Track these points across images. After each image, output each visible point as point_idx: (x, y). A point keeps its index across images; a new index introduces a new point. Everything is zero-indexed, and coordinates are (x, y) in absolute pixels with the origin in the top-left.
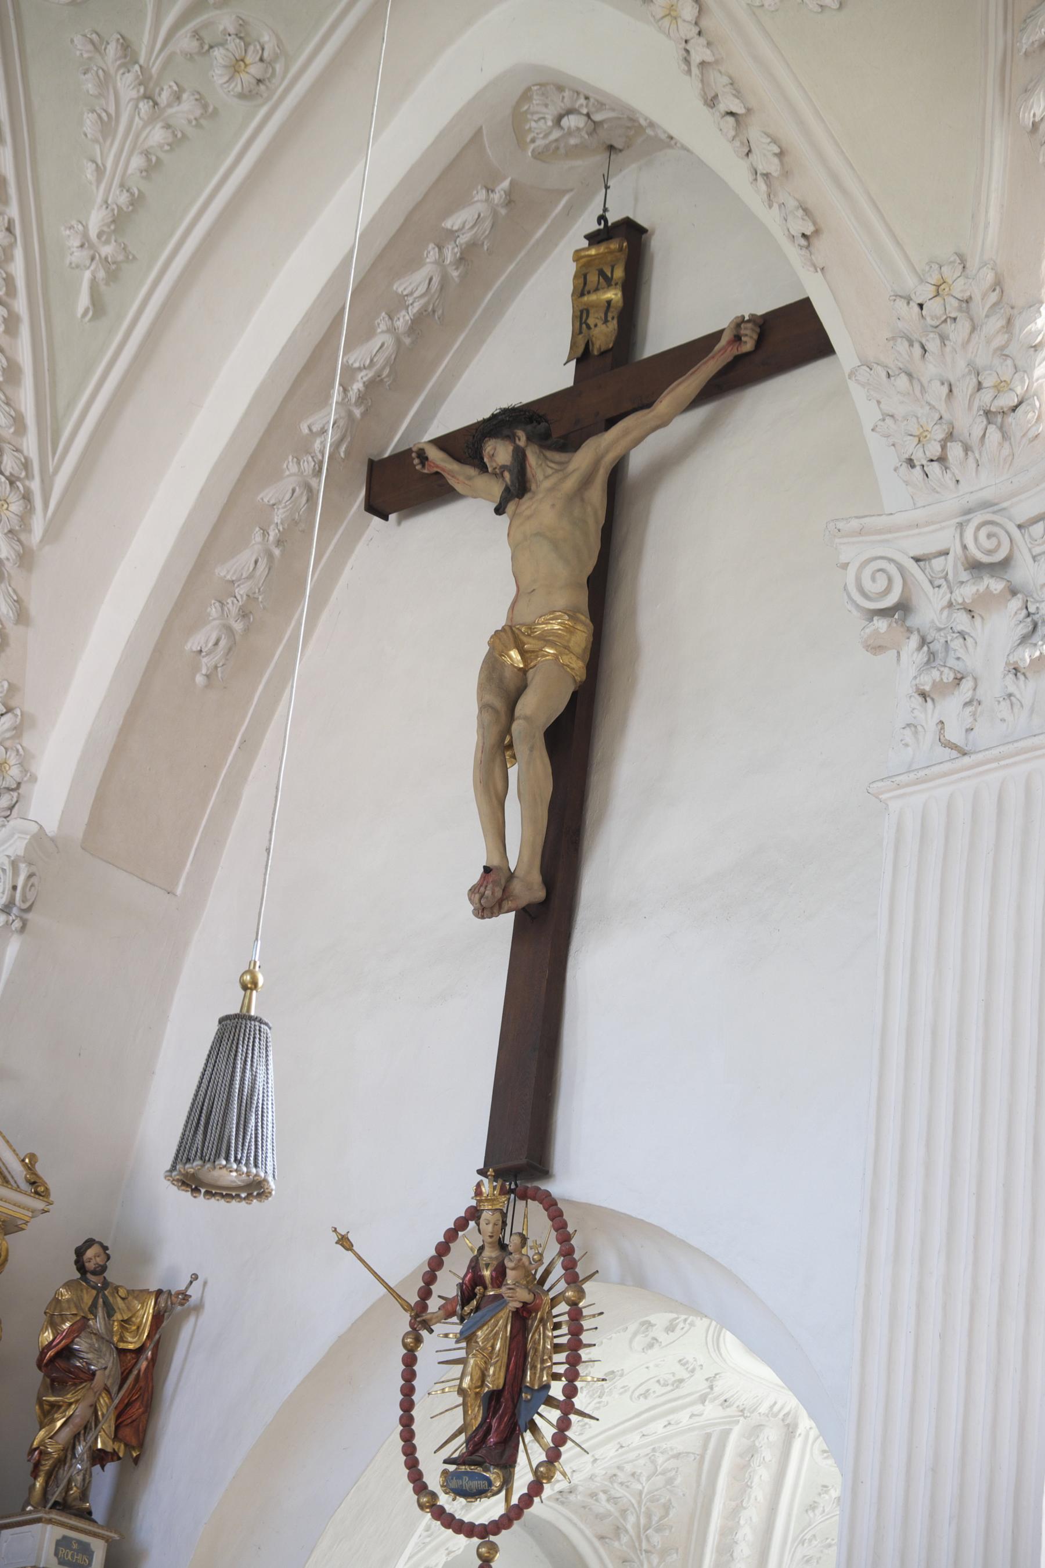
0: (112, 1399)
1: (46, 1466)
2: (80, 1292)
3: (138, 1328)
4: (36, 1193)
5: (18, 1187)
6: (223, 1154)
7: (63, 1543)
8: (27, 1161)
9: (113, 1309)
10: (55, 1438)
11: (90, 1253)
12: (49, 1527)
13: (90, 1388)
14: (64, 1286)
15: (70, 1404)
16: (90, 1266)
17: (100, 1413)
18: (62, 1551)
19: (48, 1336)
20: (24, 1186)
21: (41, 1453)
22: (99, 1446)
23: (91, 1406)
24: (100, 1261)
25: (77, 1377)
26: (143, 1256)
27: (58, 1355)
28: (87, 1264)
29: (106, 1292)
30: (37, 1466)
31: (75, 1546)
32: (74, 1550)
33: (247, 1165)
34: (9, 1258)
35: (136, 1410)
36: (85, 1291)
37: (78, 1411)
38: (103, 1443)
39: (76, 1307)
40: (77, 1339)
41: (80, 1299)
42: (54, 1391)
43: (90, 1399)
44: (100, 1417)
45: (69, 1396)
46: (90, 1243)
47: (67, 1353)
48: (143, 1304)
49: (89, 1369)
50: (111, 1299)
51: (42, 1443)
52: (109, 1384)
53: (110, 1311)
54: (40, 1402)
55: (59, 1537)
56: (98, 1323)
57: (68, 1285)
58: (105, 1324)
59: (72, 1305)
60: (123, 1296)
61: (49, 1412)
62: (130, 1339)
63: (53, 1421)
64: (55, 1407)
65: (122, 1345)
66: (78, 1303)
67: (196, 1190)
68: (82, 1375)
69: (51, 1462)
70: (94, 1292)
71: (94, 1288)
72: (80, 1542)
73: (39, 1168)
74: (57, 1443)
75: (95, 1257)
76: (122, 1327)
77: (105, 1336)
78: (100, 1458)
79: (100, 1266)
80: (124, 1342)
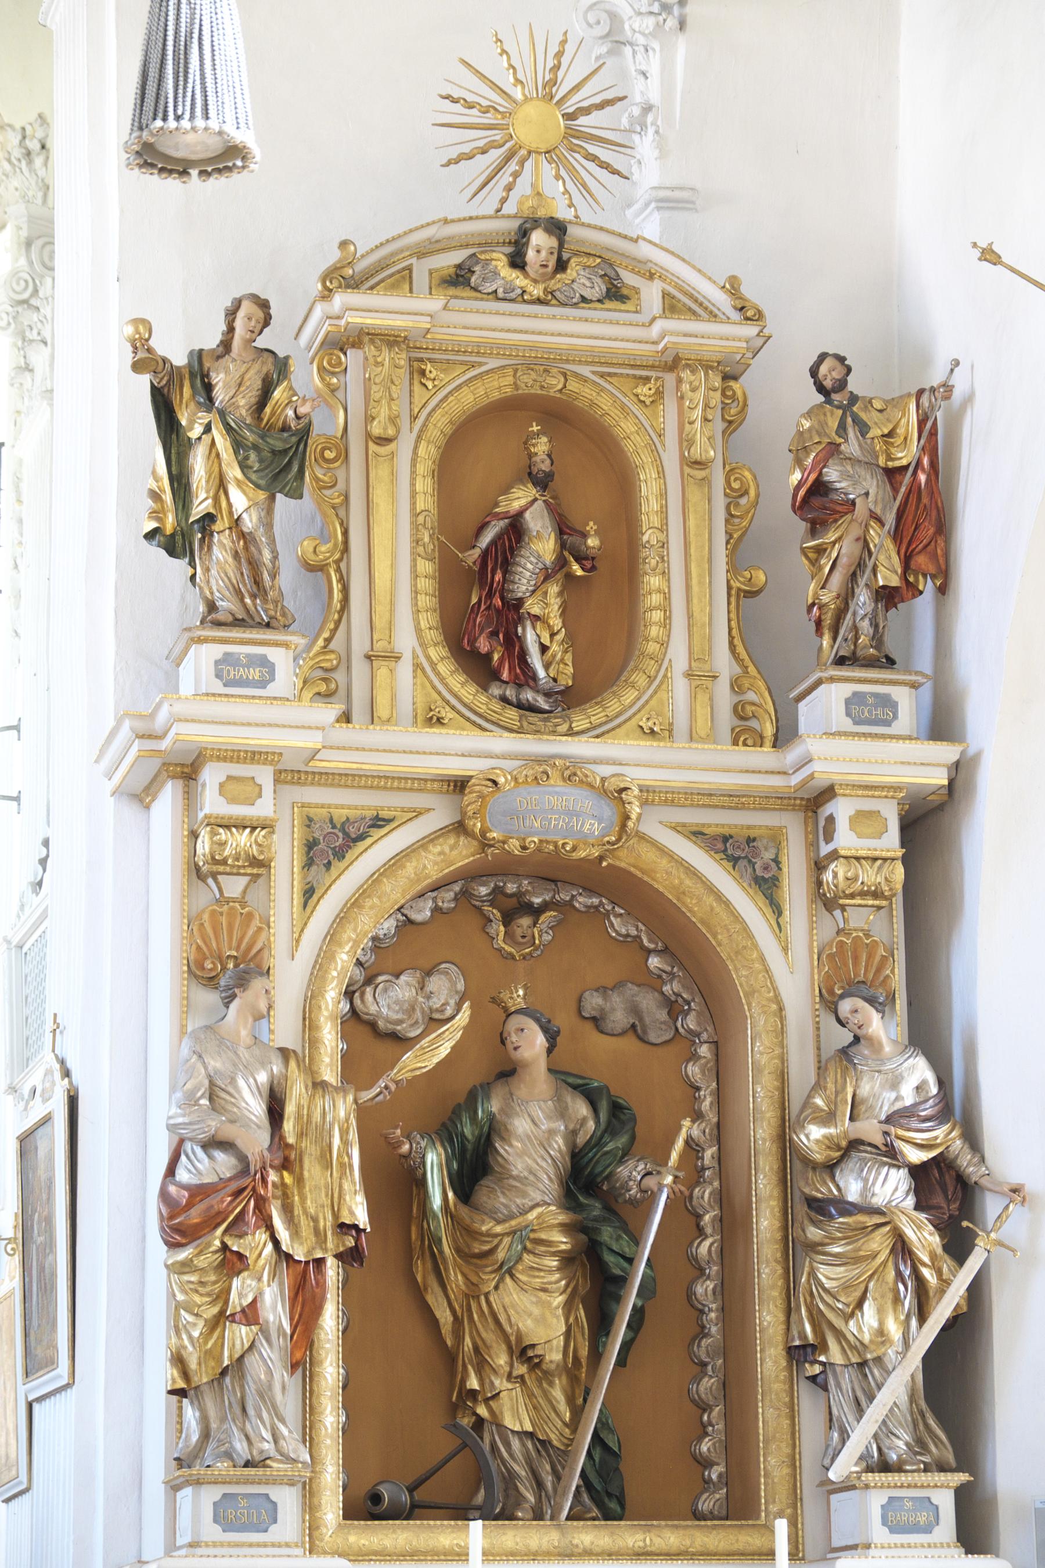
0: (883, 524)
1: (828, 620)
2: (822, 417)
3: (906, 439)
4: (747, 319)
5: (728, 318)
6: (160, 115)
7: (853, 702)
8: (728, 286)
9: (866, 425)
10: (828, 586)
11: (823, 369)
12: (833, 686)
13: (852, 520)
14: (803, 416)
15: (834, 543)
16: (828, 384)
17: (871, 546)
18: (855, 709)
19: (797, 476)
20: (735, 316)
21: (820, 608)
22: (881, 583)
23: (858, 539)
24: (836, 375)
25: (836, 512)
26: (924, 359)
27: (810, 492)
28: (824, 383)
29: (855, 409)
30: (819, 623)
31: (870, 700)
32: (871, 705)
33: (178, 118)
34: (749, 402)
35: (928, 531)
36: (828, 414)
37: (848, 549)
38: (885, 578)
39: (819, 434)
40: (825, 470)
41: (823, 424)
42: (813, 532)
43: (856, 531)
44: (873, 549)
45: (830, 534)
46: (823, 357)
47: (819, 488)
48: (905, 412)
49: (848, 499)
50: (863, 415)
51: (816, 596)
52: (878, 511)
53: (863, 429)
54: (804, 551)
55: (849, 694)
56: (852, 446)
57: (808, 414)
58: (860, 445)
59: (814, 433)
60: (879, 407)
61: (817, 560)
62: (900, 455)
63: (821, 568)
64: (820, 551)
65: (890, 464)
66: (820, 429)
67: (184, 173)
68: (839, 508)
69: (830, 614)
70: (840, 412)
71: (838, 407)
72: (876, 695)
73: (746, 290)
74: (830, 591)
75: (830, 372)
76: (886, 443)
77: (862, 458)
78: (887, 597)
79: (840, 380)
80: (893, 460)
